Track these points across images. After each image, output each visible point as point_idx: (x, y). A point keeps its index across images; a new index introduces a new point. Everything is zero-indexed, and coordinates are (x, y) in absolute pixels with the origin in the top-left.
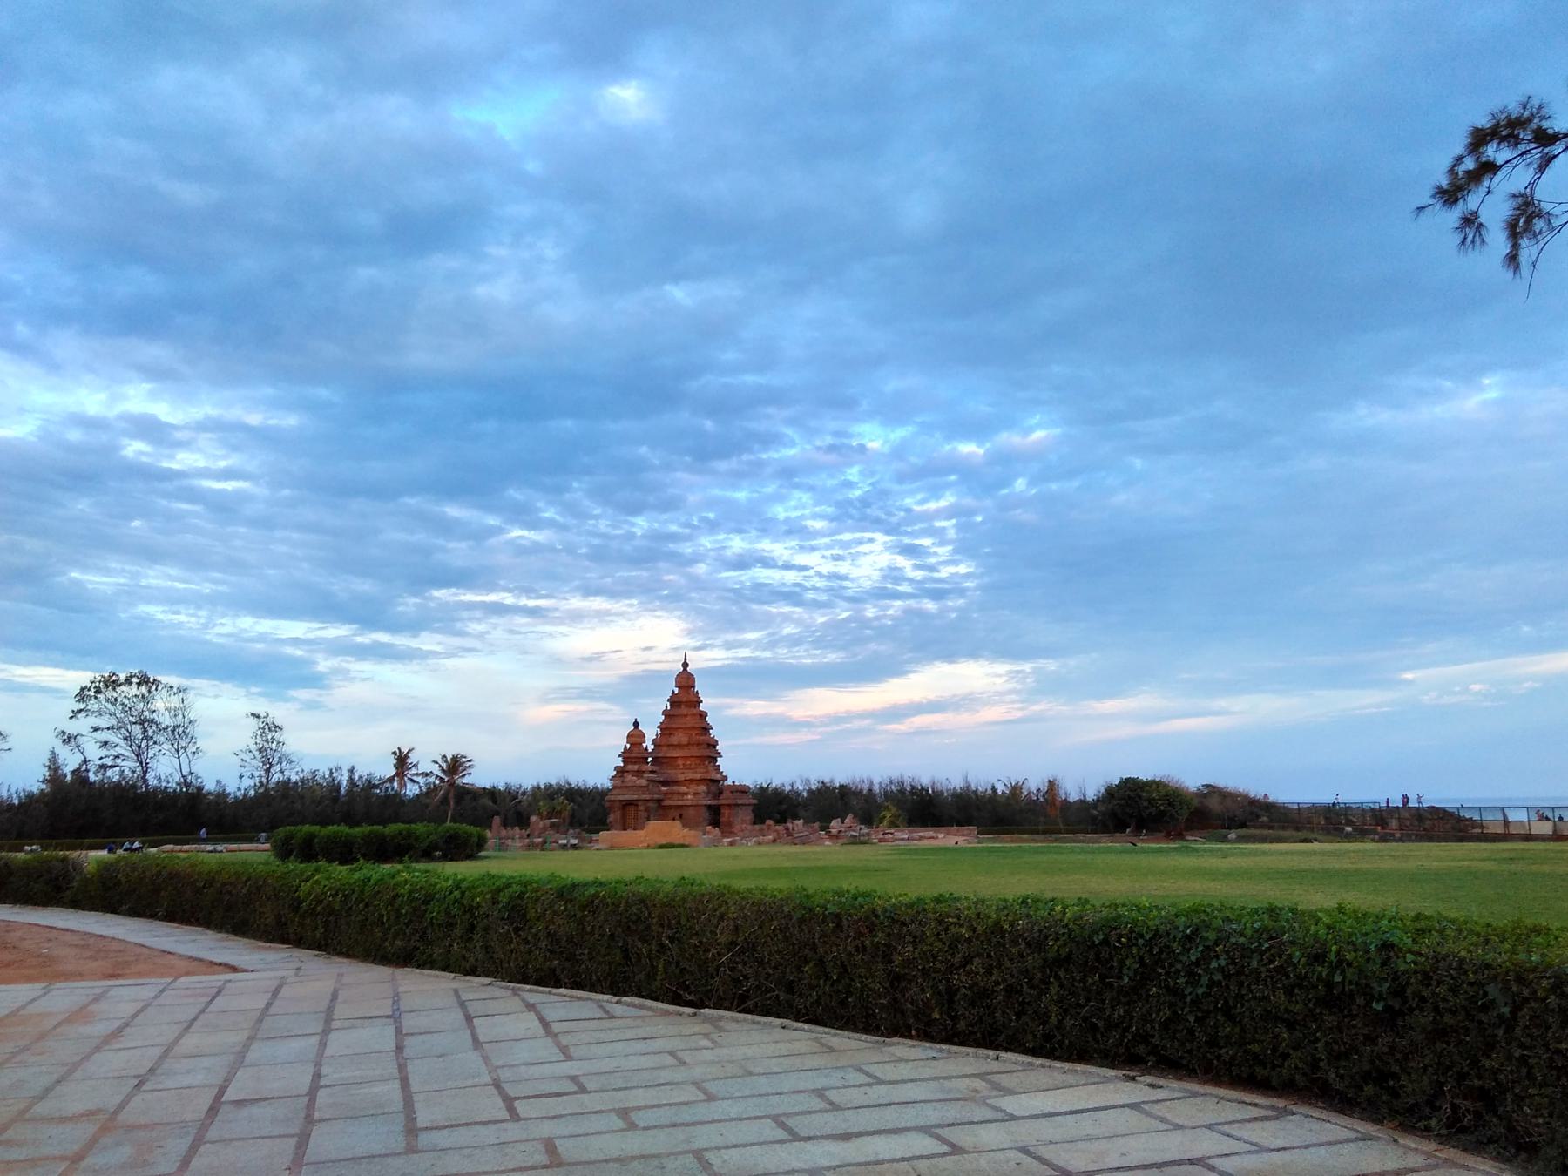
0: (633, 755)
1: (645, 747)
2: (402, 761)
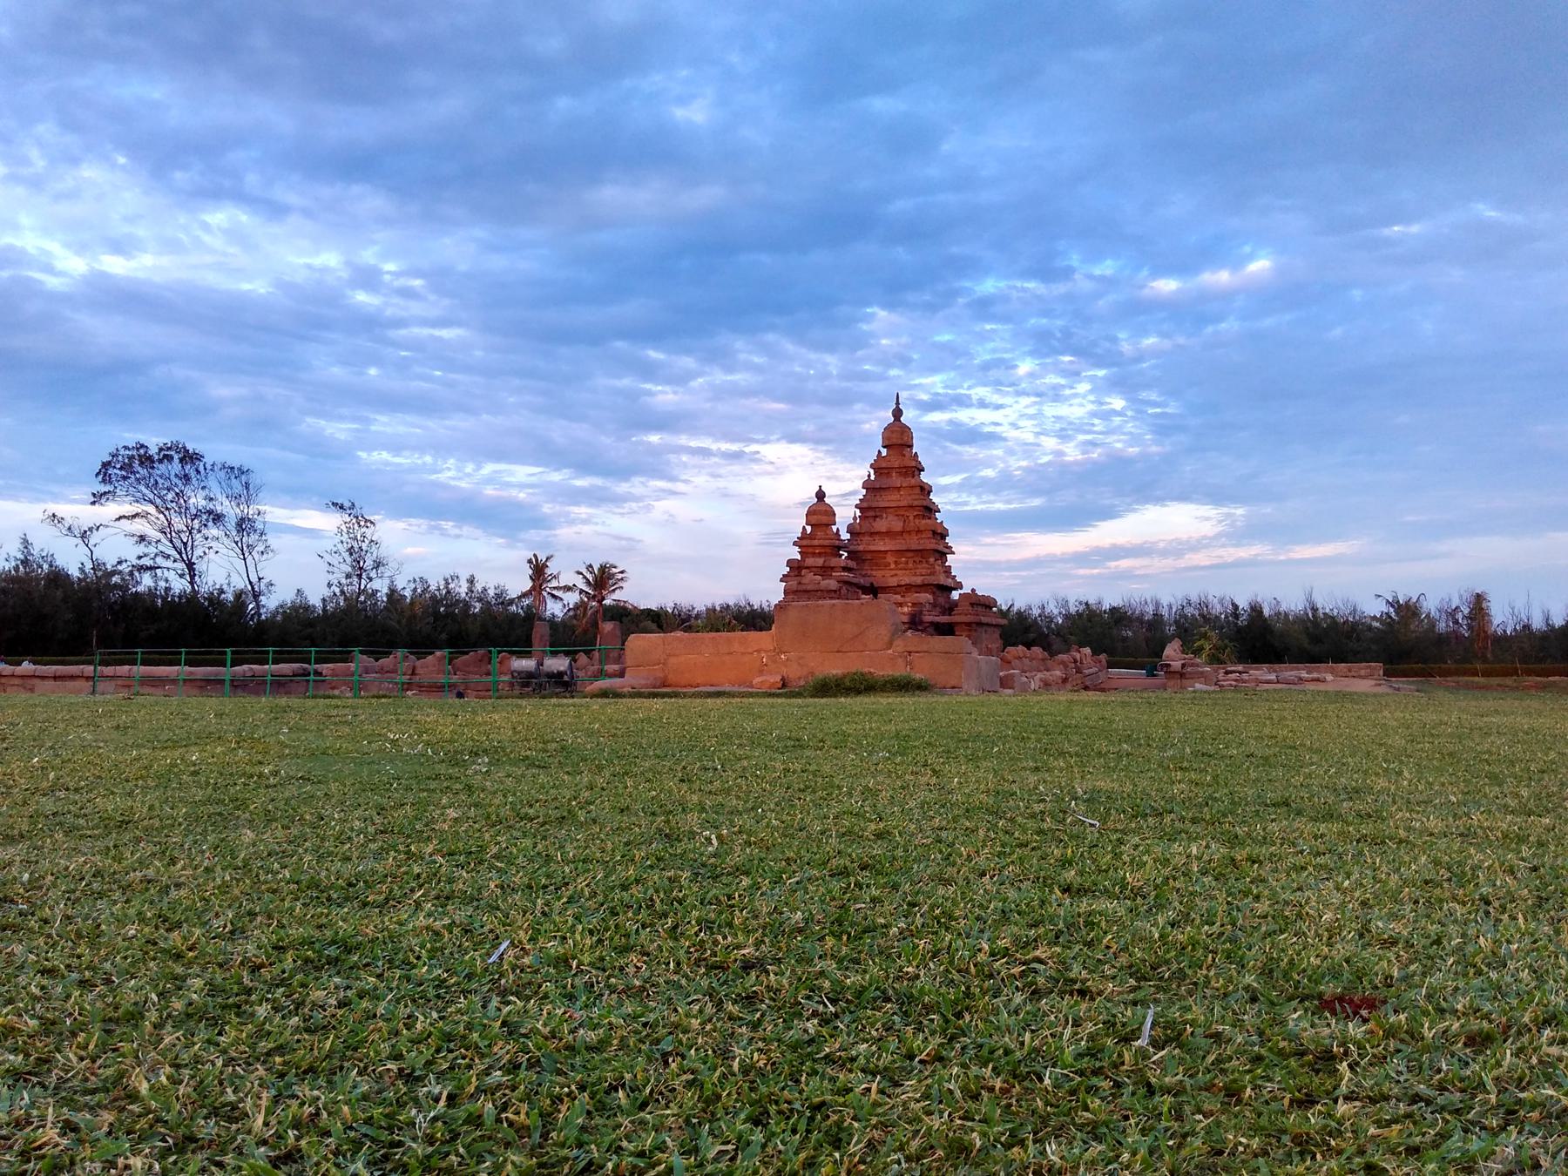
0: (816, 542)
1: (835, 531)
2: (539, 571)
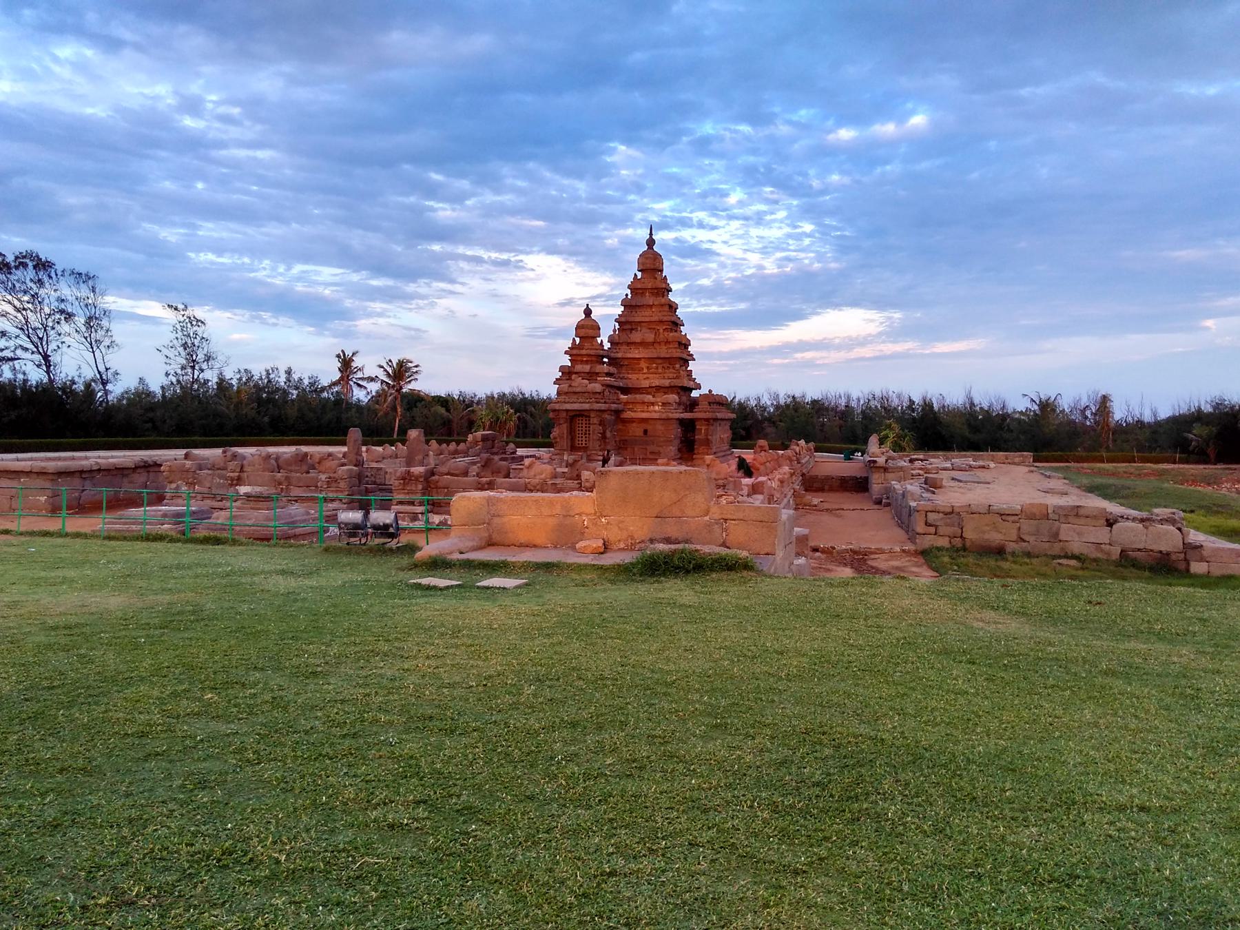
0: (584, 352)
1: (599, 342)
2: (346, 364)
